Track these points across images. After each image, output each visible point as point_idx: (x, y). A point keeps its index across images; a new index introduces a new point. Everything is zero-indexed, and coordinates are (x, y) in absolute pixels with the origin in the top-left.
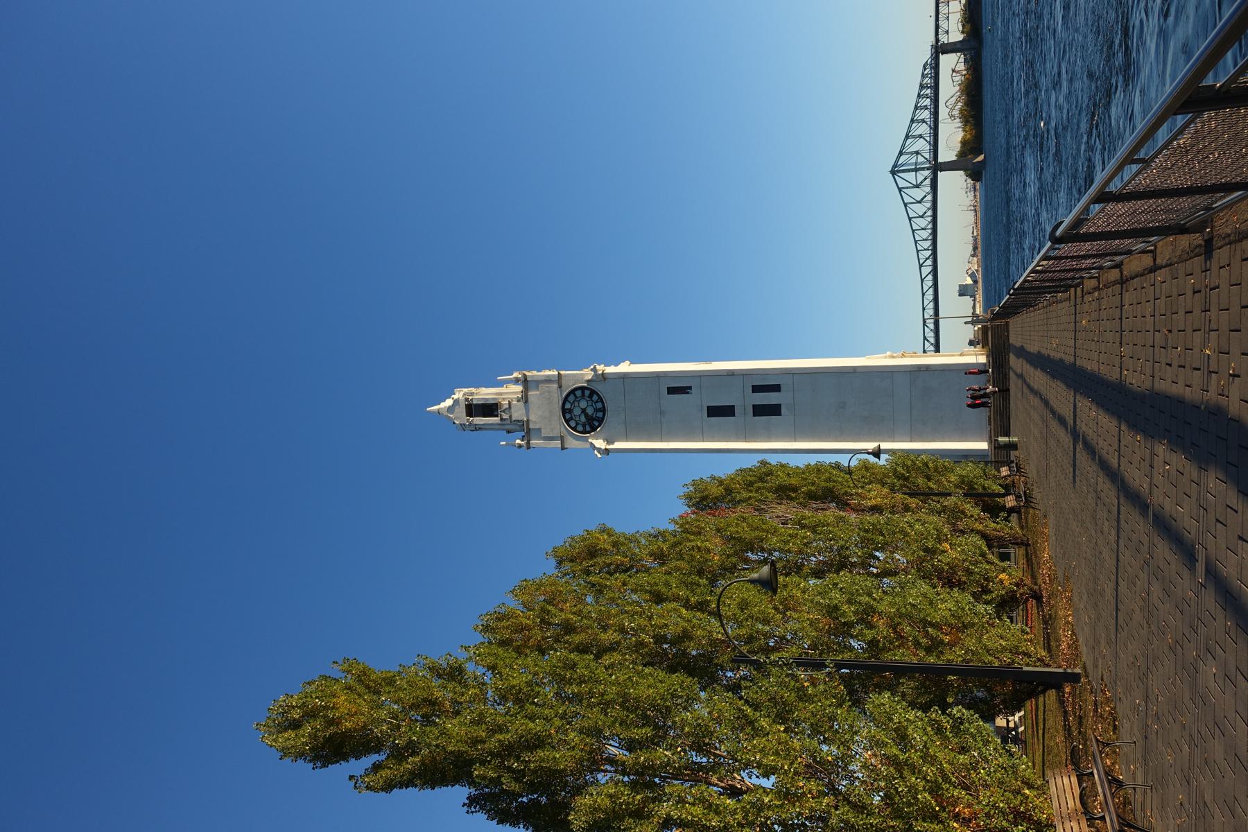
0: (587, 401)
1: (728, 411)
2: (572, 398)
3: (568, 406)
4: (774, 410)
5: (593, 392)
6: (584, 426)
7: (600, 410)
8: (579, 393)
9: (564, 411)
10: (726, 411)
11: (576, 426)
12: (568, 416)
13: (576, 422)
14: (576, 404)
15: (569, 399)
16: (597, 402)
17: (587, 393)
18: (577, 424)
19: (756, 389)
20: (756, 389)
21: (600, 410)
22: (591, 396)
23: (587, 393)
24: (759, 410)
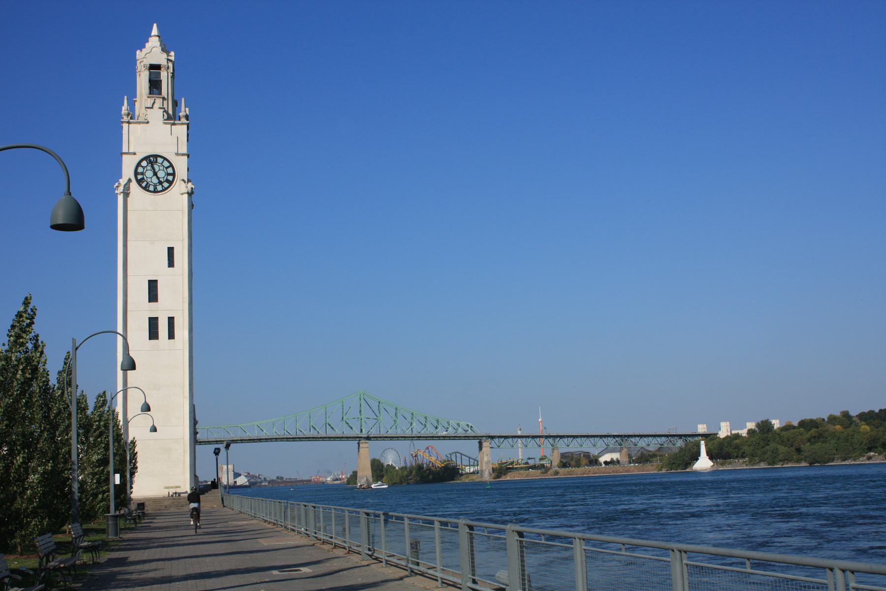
0: (164, 177)
1: (153, 296)
2: (166, 164)
3: (160, 160)
4: (153, 334)
6: (142, 174)
7: (155, 188)
8: (170, 170)
9: (156, 156)
10: (153, 296)
11: (141, 166)
13: (145, 167)
14: (162, 168)
15: (165, 161)
17: (170, 178)
18: (144, 167)
19: (171, 320)
20: (171, 320)
21: (155, 188)
22: (167, 181)
23: (170, 178)
24: (153, 323)
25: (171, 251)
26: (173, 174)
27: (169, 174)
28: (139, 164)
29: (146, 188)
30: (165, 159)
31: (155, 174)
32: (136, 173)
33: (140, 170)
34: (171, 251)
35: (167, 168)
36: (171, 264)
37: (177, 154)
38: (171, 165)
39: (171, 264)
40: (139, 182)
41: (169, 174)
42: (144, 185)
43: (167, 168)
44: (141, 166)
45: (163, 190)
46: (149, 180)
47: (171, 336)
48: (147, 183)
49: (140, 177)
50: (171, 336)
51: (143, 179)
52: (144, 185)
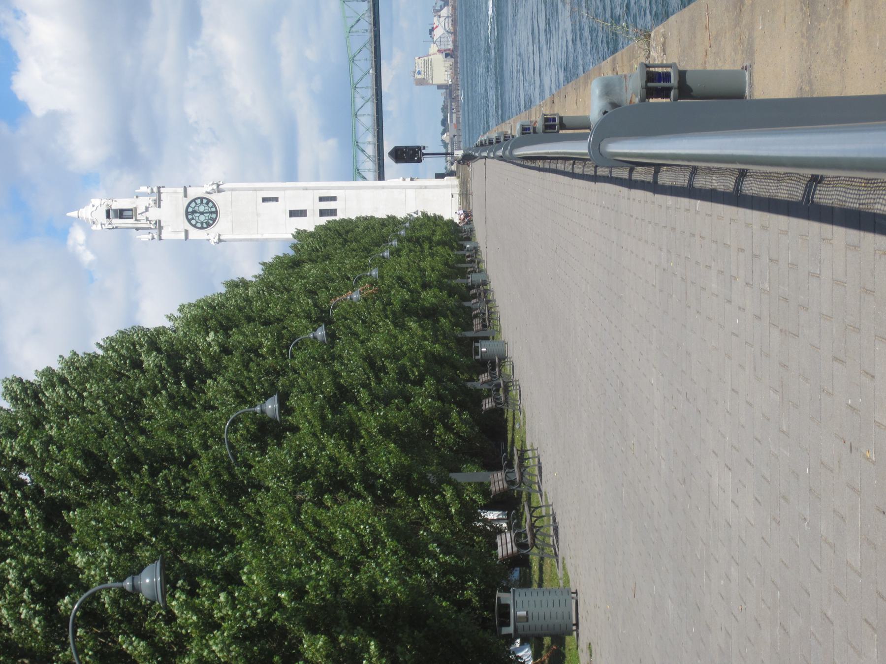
1: (302, 213)
2: (193, 205)
5: (209, 201)
6: (202, 223)
8: (198, 201)
9: (187, 213)
11: (196, 224)
12: (190, 217)
16: (212, 207)
17: (205, 201)
18: (197, 222)
19: (321, 199)
20: (321, 199)
22: (207, 203)
23: (205, 201)
25: (265, 200)
26: (202, 199)
27: (202, 202)
28: (195, 226)
29: (214, 220)
30: (189, 205)
31: (202, 213)
32: (202, 228)
33: (199, 225)
34: (265, 200)
35: (196, 204)
36: (276, 199)
37: (186, 196)
38: (194, 200)
39: (276, 199)
40: (209, 225)
41: (202, 202)
42: (211, 222)
43: (196, 204)
44: (196, 224)
45: (215, 207)
46: (207, 218)
47: (334, 199)
48: (210, 219)
49: (205, 225)
50: (334, 199)
51: (206, 223)
52: (211, 222)
